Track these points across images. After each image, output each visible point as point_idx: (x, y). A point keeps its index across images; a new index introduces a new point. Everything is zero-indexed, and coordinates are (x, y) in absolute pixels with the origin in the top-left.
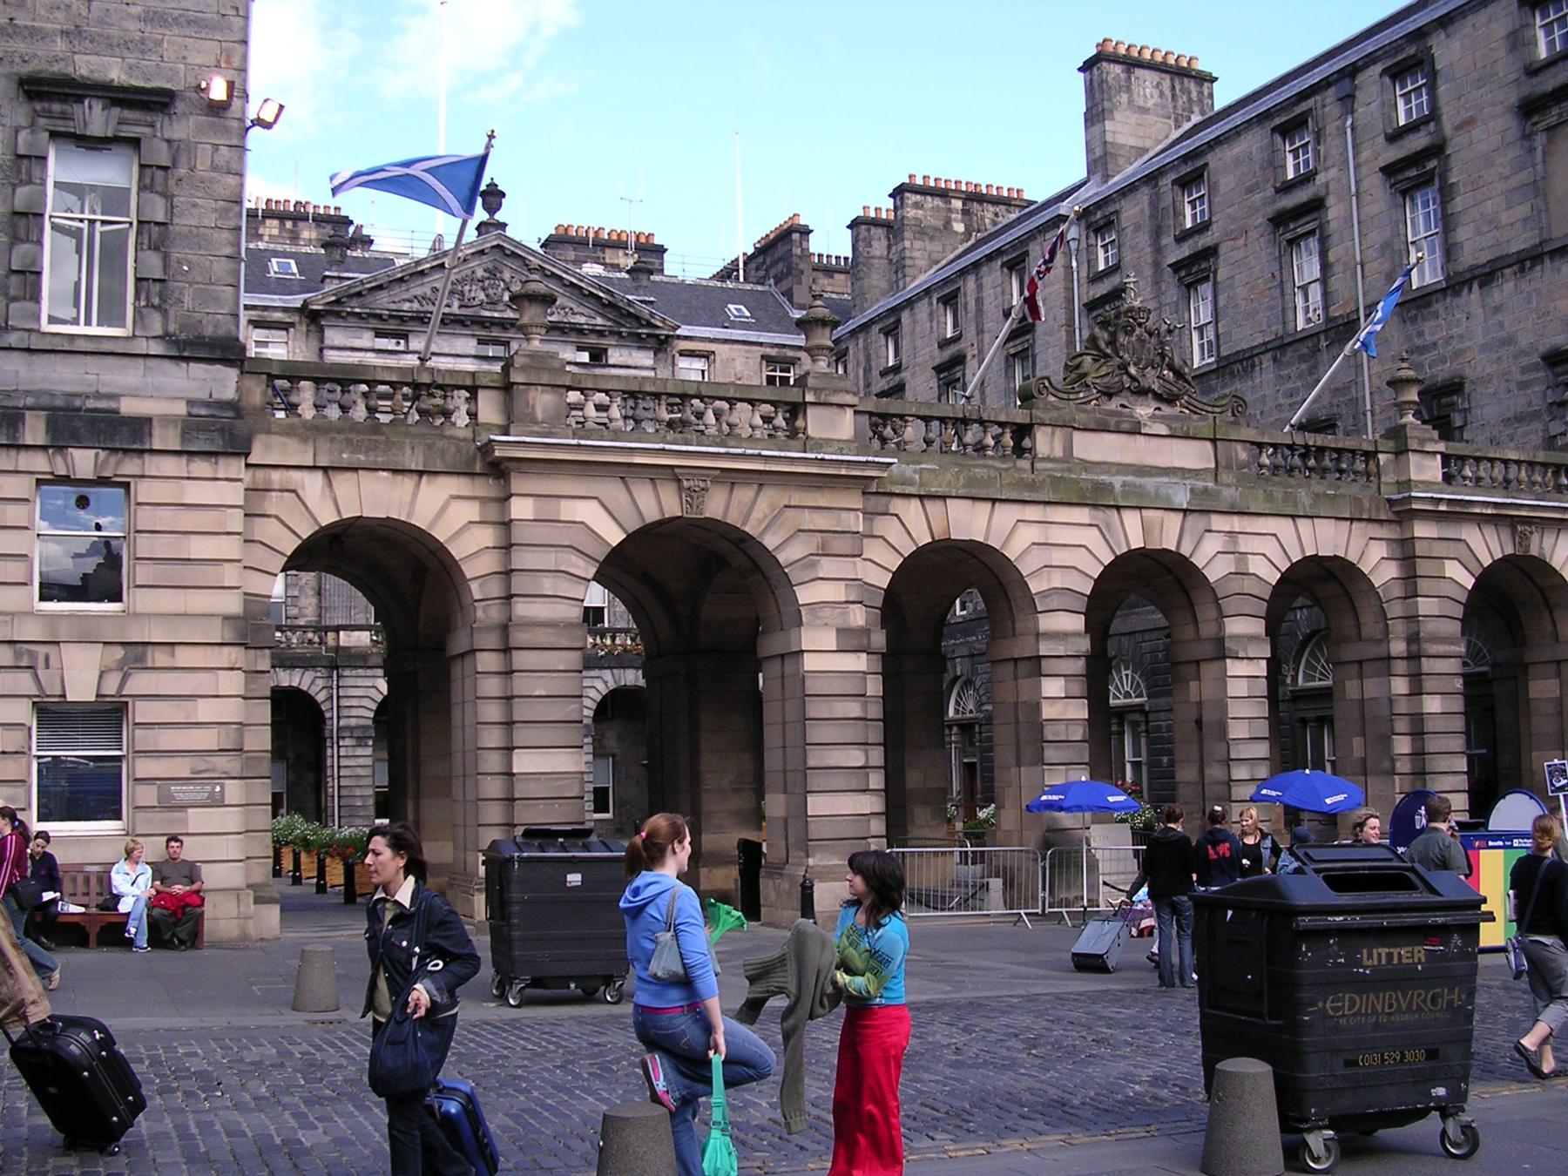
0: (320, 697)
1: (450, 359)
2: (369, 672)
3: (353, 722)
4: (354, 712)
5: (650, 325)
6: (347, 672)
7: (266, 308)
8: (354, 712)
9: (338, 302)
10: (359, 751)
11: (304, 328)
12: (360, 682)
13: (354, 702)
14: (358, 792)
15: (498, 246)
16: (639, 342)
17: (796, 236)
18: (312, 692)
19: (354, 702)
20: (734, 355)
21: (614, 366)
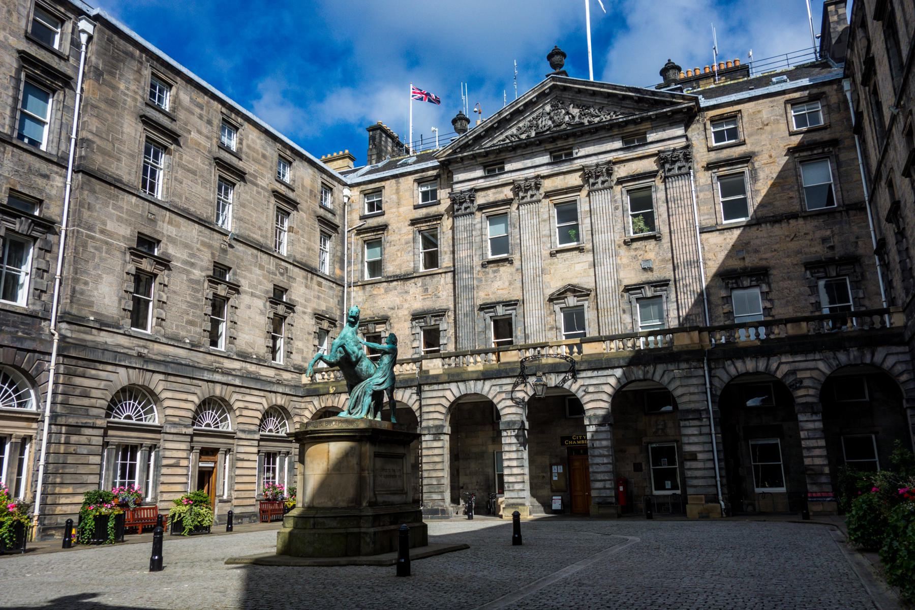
0: (415, 407)
1: (532, 170)
2: (441, 387)
3: (431, 423)
4: (431, 416)
5: (673, 104)
6: (426, 388)
7: (423, 170)
8: (431, 416)
9: (454, 152)
10: (436, 444)
11: (446, 176)
12: (435, 394)
13: (432, 409)
14: (434, 474)
15: (554, 87)
16: (671, 120)
17: (831, 8)
18: (410, 403)
19: (432, 409)
20: (760, 108)
21: (652, 143)
